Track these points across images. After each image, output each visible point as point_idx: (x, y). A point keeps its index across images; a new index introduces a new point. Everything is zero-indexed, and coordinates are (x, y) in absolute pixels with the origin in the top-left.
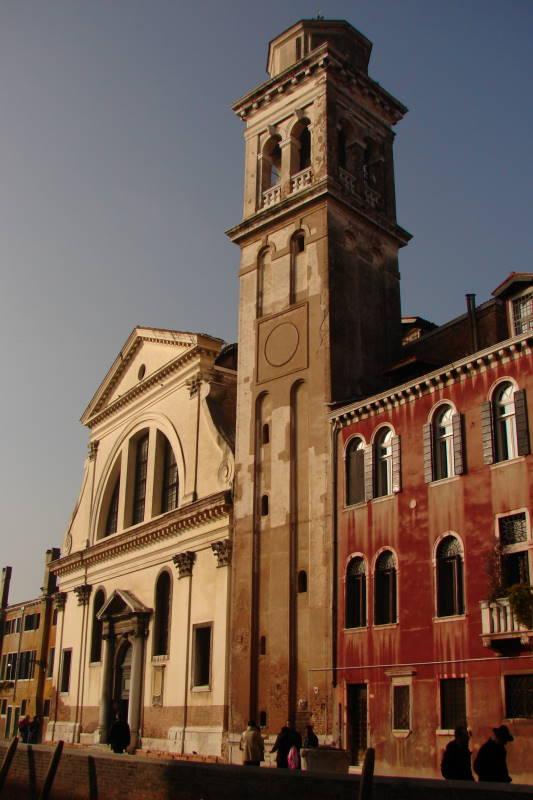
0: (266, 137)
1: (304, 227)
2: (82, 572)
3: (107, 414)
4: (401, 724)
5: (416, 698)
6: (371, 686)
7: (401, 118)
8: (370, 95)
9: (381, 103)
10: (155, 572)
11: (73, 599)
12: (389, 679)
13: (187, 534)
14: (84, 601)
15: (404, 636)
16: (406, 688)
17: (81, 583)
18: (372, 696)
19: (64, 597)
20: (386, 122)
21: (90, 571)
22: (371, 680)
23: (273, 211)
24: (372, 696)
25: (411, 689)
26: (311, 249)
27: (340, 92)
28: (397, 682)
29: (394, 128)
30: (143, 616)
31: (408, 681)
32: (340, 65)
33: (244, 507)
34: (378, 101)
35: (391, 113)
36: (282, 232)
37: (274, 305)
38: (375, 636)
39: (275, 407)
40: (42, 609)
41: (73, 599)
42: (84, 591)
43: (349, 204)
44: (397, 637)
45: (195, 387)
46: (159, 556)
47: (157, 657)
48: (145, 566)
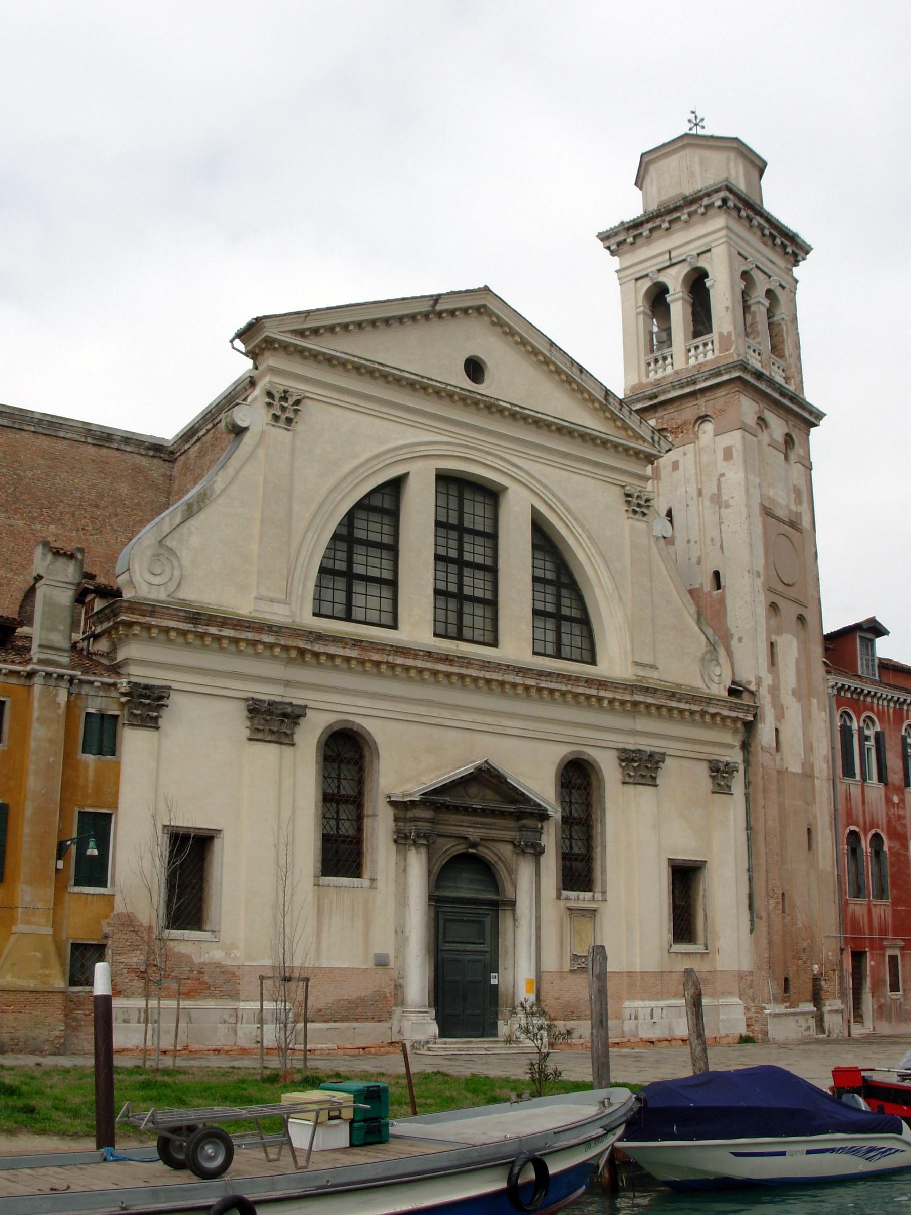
0: (646, 285)
4: (895, 987)
5: (903, 966)
6: (871, 954)
12: (883, 948)
15: (895, 913)
16: (897, 956)
18: (873, 963)
22: (872, 948)
24: (873, 963)
25: (899, 958)
28: (889, 952)
31: (897, 952)
38: (873, 909)
44: (889, 912)
46: (571, 731)
47: (565, 893)
48: (540, 735)
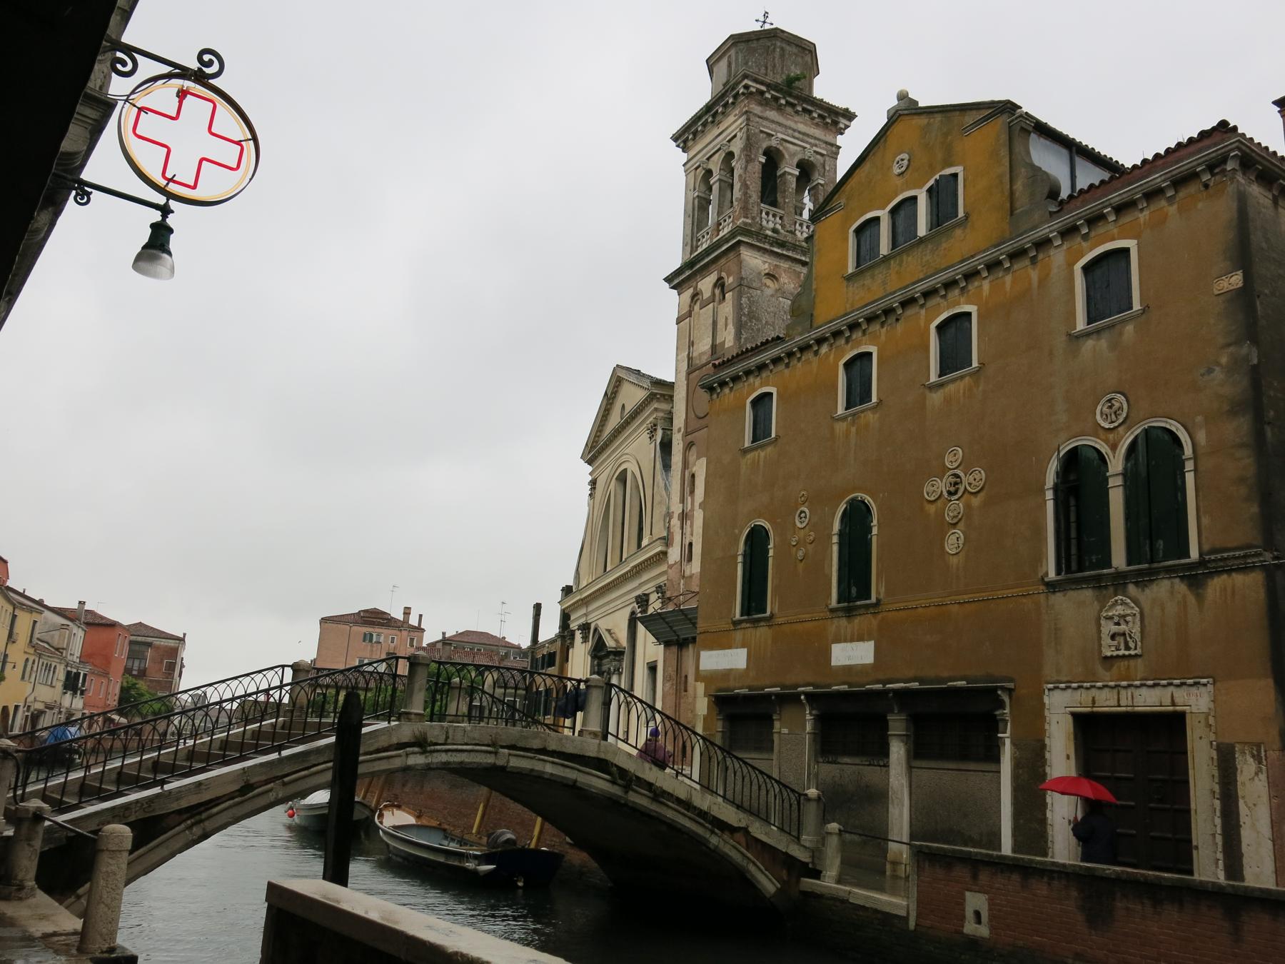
0: (701, 172)
1: (724, 274)
2: (583, 611)
3: (603, 449)
7: (847, 127)
8: (805, 110)
9: (820, 116)
10: (627, 611)
11: (578, 635)
13: (645, 577)
14: (585, 639)
17: (582, 621)
19: (572, 634)
20: (829, 138)
21: (590, 608)
23: (707, 252)
26: (729, 296)
27: (766, 119)
29: (840, 140)
30: (618, 653)
32: (763, 88)
33: (674, 554)
34: (815, 115)
35: (835, 123)
36: (708, 279)
37: (701, 354)
39: (698, 458)
40: (557, 647)
41: (578, 635)
42: (585, 628)
43: (767, 246)
45: (653, 430)
